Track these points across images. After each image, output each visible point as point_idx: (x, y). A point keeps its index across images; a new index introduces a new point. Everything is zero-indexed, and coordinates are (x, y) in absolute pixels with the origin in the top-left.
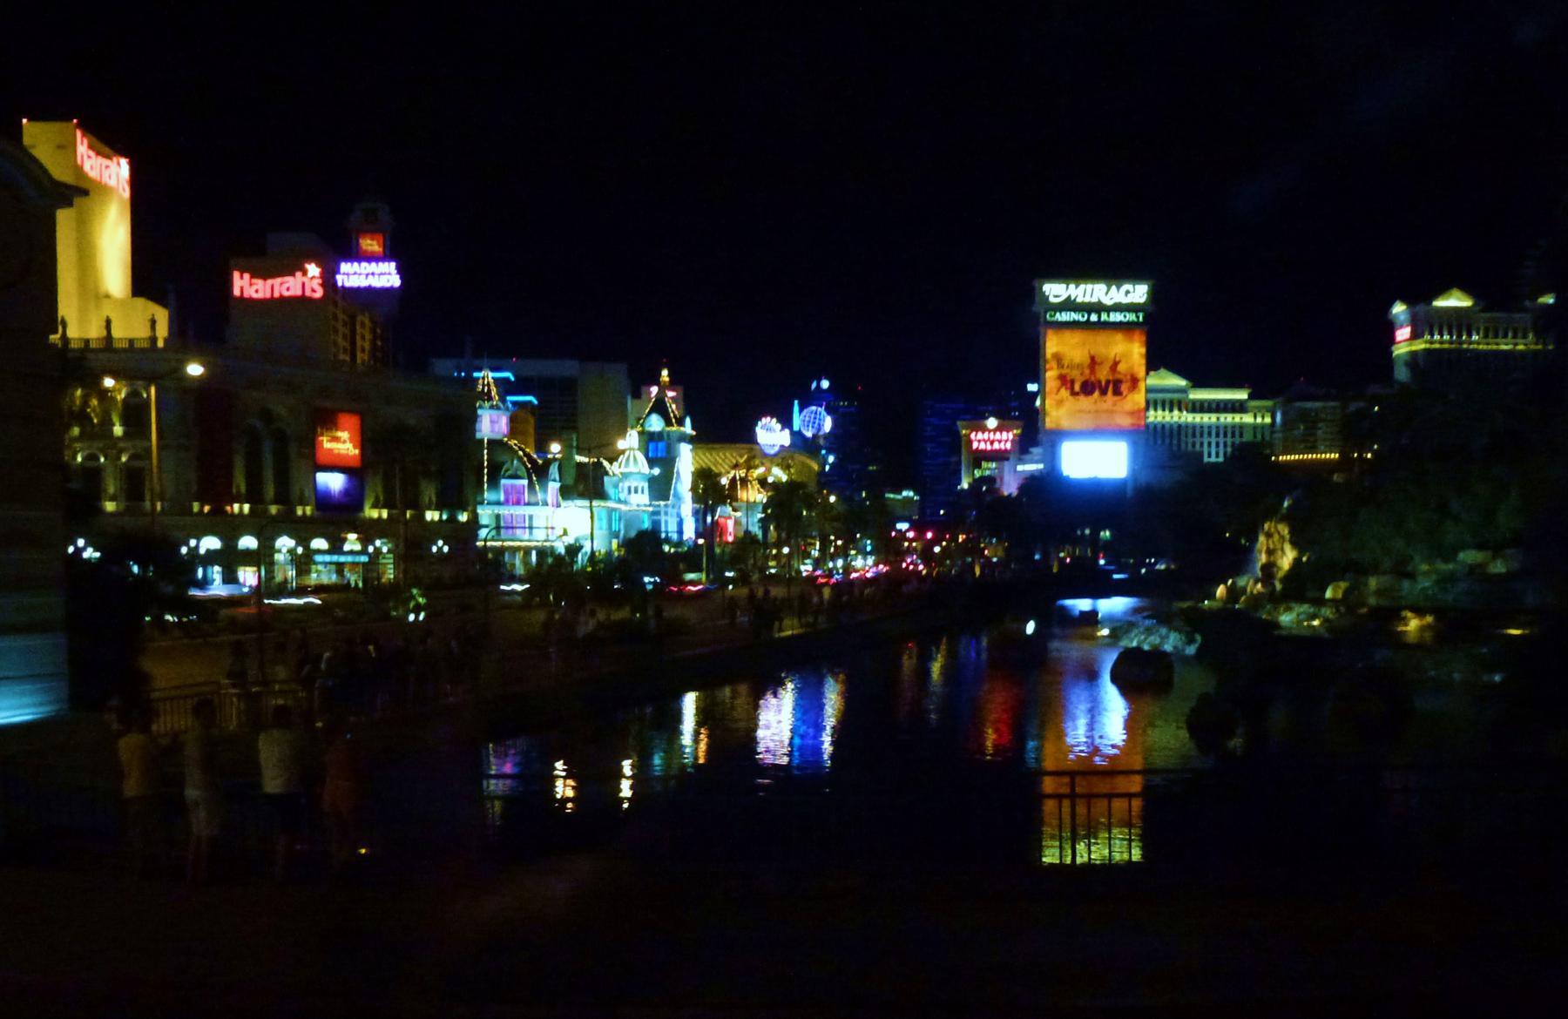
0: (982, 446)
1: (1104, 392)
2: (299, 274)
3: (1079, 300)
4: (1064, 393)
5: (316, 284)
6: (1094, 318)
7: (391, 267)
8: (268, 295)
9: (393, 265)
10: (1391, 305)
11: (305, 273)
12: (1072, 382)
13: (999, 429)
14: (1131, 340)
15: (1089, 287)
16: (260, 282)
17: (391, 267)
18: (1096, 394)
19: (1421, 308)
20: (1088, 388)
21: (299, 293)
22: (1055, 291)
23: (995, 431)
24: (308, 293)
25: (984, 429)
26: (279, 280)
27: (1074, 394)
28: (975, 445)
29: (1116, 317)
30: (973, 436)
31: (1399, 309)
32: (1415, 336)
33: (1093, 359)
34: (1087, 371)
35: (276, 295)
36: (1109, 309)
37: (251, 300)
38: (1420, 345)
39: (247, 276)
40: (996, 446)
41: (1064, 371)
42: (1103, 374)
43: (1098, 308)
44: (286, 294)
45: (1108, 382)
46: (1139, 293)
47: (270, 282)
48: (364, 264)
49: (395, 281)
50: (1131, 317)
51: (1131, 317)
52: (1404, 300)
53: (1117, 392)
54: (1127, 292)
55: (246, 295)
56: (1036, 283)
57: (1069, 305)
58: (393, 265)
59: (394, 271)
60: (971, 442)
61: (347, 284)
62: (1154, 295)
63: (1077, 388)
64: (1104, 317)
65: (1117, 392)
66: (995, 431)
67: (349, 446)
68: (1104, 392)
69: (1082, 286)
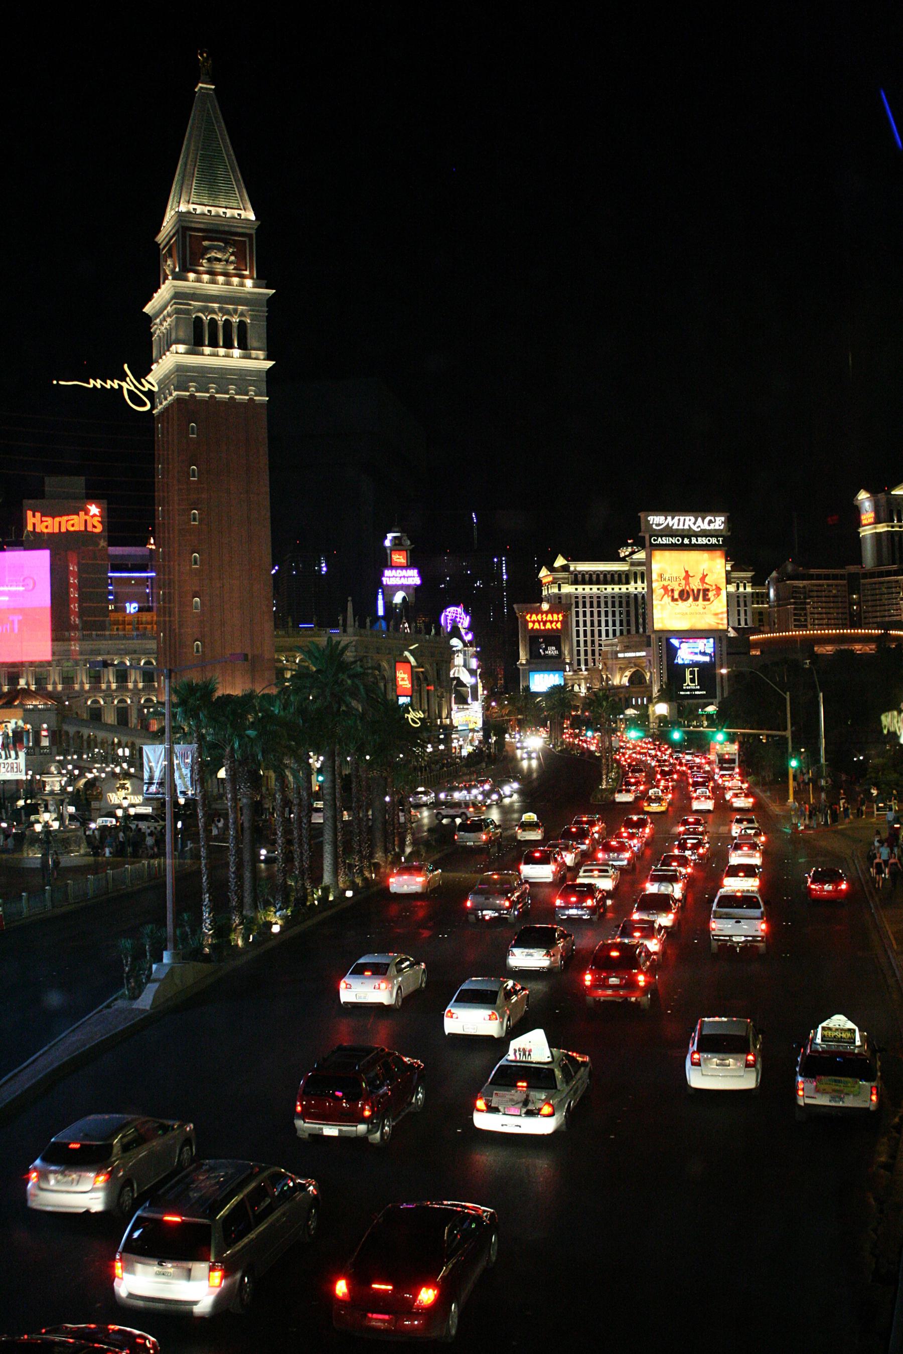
0: (537, 626)
1: (696, 599)
2: (82, 513)
3: (675, 527)
4: (667, 599)
5: (96, 521)
6: (686, 541)
7: (414, 572)
8: (56, 530)
9: (416, 571)
10: (857, 493)
11: (87, 512)
12: (672, 591)
13: (551, 611)
14: (712, 559)
15: (682, 518)
16: (49, 519)
17: (414, 572)
18: (691, 599)
19: (881, 496)
20: (684, 595)
21: (83, 528)
22: (657, 521)
23: (547, 613)
24: (90, 529)
25: (539, 611)
26: (65, 518)
27: (674, 600)
28: (530, 625)
29: (703, 541)
30: (528, 617)
31: (863, 495)
32: (878, 521)
33: (687, 572)
34: (683, 582)
35: (63, 530)
36: (697, 536)
37: (42, 534)
38: (882, 528)
39: (38, 515)
40: (548, 626)
41: (666, 583)
42: (695, 584)
43: (689, 534)
44: (72, 529)
45: (699, 590)
46: (718, 523)
47: (57, 519)
48: (399, 571)
49: (417, 581)
50: (714, 541)
51: (714, 541)
52: (867, 490)
53: (706, 599)
54: (710, 522)
55: (38, 530)
56: (642, 515)
57: (669, 532)
58: (416, 571)
59: (416, 575)
60: (527, 622)
61: (389, 583)
62: (728, 522)
63: (676, 596)
64: (694, 541)
65: (706, 599)
66: (547, 613)
67: (407, 682)
68: (696, 599)
69: (676, 518)
